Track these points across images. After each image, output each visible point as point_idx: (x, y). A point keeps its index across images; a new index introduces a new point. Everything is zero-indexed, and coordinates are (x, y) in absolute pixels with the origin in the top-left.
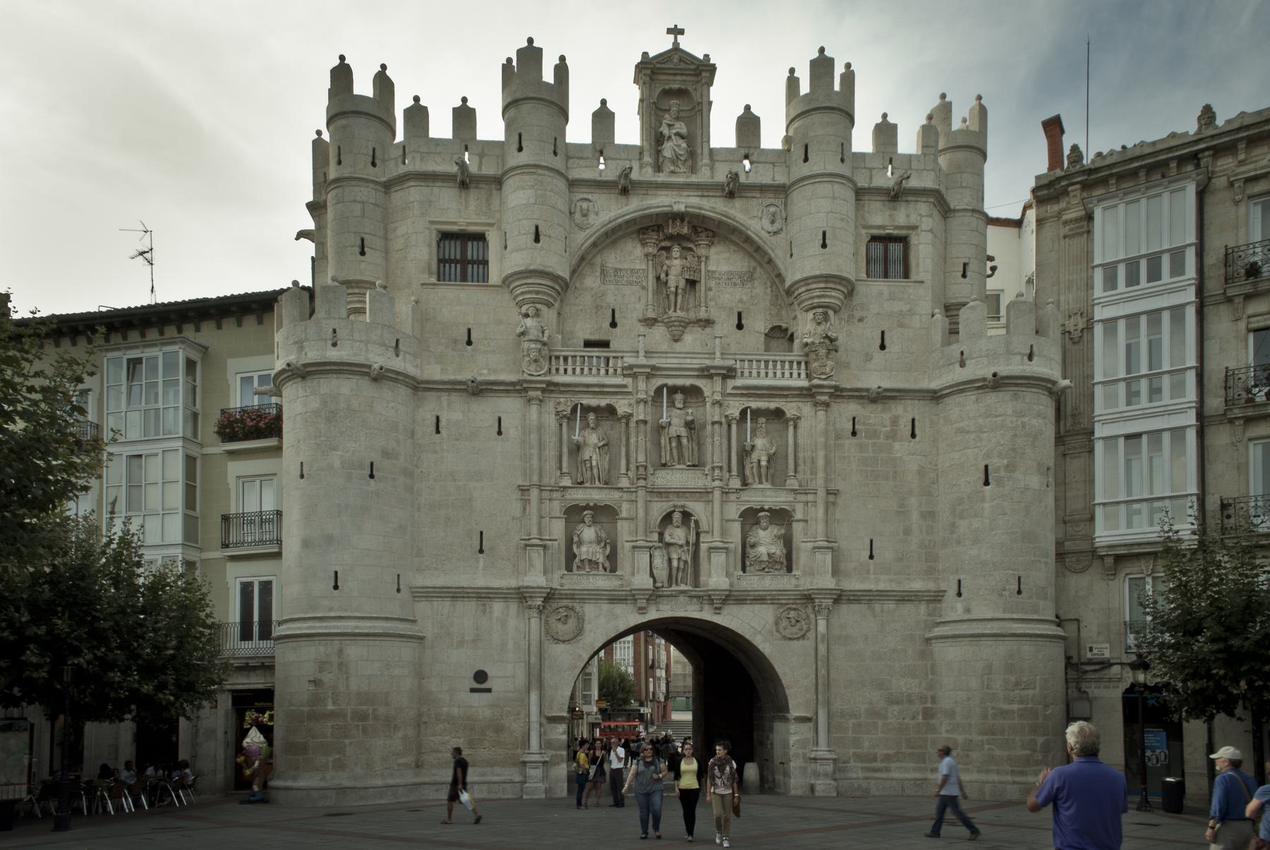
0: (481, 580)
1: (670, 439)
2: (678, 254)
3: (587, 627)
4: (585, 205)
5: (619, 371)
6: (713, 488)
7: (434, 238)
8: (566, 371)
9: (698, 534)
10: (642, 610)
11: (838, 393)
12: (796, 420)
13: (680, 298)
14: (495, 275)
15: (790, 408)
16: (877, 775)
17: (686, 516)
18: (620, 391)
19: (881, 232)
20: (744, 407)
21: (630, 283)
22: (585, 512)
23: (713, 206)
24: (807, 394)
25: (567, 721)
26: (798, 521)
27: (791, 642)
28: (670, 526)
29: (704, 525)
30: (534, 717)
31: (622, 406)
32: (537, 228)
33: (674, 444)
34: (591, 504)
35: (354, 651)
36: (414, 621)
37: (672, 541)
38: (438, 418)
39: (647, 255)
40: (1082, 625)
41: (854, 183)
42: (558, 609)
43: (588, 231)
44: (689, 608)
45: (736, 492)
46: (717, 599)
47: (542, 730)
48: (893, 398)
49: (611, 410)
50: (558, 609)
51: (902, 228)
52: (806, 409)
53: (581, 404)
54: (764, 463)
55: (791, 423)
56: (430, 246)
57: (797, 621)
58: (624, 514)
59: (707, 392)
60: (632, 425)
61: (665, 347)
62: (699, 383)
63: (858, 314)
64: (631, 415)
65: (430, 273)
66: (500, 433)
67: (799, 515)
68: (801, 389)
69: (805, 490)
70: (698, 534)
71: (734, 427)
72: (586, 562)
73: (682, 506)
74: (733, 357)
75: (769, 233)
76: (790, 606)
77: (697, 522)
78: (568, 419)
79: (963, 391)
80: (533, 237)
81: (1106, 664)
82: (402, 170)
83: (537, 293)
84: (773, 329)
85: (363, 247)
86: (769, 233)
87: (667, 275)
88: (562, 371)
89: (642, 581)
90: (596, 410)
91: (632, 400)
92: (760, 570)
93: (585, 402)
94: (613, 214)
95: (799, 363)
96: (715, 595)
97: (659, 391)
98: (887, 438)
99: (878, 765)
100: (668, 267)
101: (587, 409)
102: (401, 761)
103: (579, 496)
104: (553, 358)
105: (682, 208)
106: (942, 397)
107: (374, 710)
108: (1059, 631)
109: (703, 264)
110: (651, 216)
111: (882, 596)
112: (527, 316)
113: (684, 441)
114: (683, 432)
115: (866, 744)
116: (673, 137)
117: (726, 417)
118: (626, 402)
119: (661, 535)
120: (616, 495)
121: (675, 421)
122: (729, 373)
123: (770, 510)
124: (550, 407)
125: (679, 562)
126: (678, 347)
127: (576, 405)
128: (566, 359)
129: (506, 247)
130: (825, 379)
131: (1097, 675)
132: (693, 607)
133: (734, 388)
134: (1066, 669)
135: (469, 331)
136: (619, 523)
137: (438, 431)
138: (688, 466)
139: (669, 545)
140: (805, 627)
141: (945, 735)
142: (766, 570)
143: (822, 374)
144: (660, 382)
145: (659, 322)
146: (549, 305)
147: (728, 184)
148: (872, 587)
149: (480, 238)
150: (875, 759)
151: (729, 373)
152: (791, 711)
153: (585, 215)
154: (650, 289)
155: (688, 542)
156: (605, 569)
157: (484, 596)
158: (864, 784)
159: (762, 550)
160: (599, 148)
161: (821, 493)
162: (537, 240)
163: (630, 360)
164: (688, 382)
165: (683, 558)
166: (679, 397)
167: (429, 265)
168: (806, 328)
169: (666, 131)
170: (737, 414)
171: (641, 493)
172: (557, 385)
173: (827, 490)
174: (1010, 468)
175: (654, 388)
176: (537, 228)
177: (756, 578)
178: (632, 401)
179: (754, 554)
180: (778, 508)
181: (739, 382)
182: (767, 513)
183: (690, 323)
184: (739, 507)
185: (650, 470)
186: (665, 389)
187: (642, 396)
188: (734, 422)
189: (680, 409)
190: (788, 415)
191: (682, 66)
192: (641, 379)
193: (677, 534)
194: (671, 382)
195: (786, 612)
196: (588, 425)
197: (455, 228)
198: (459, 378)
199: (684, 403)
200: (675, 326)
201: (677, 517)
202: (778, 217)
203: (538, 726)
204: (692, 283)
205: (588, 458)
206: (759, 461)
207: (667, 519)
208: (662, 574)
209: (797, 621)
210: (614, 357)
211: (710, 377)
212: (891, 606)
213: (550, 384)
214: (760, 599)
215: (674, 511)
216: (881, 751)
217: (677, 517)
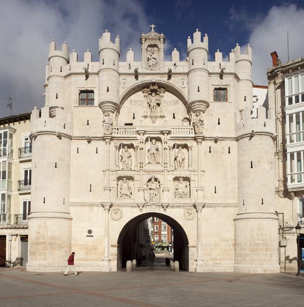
0: (90, 200)
3: (123, 216)
4: (124, 80)
7: (78, 92)
9: (160, 185)
11: (204, 139)
14: (96, 103)
15: (189, 143)
16: (217, 265)
17: (156, 180)
18: (135, 139)
19: (218, 87)
21: (139, 105)
23: (164, 80)
24: (195, 139)
27: (190, 221)
30: (107, 245)
31: (135, 143)
33: (152, 155)
35: (49, 222)
36: (70, 214)
38: (78, 148)
40: (284, 215)
41: (208, 72)
48: (223, 140)
51: (224, 85)
52: (194, 143)
54: (181, 162)
56: (76, 95)
58: (135, 179)
60: (139, 148)
61: (150, 125)
62: (160, 136)
63: (211, 113)
65: (76, 103)
66: (97, 153)
67: (192, 179)
68: (192, 137)
70: (160, 185)
79: (244, 137)
81: (291, 228)
82: (69, 72)
84: (184, 119)
85: (57, 96)
88: (116, 133)
89: (141, 201)
91: (139, 142)
93: (124, 143)
94: (133, 84)
95: (192, 129)
98: (221, 153)
99: (217, 262)
102: (64, 258)
103: (122, 174)
105: (154, 81)
106: (239, 140)
107: (55, 242)
108: (276, 217)
110: (145, 83)
111: (219, 205)
113: (155, 155)
114: (155, 152)
115: (214, 255)
119: (147, 185)
121: (152, 148)
122: (169, 133)
123: (183, 177)
124: (113, 143)
126: (154, 125)
128: (118, 129)
131: (289, 231)
132: (157, 209)
134: (279, 229)
137: (78, 153)
139: (150, 189)
141: (238, 252)
144: (147, 136)
146: (113, 113)
148: (216, 203)
149: (92, 92)
150: (216, 260)
151: (169, 133)
152: (189, 244)
153: (124, 84)
157: (92, 205)
158: (213, 268)
159: (180, 191)
161: (200, 171)
163: (138, 129)
164: (156, 136)
166: (154, 141)
167: (76, 101)
168: (194, 117)
169: (150, 58)
170: (172, 146)
171: (141, 171)
172: (115, 137)
174: (259, 162)
181: (172, 135)
185: (144, 164)
187: (142, 140)
190: (189, 146)
191: (155, 37)
192: (141, 135)
193: (154, 185)
194: (151, 136)
197: (84, 89)
198: (85, 135)
201: (153, 180)
202: (185, 83)
204: (159, 105)
207: (150, 180)
208: (147, 199)
211: (163, 134)
212: (222, 209)
213: (112, 137)
214: (179, 207)
216: (219, 257)
217: (153, 180)
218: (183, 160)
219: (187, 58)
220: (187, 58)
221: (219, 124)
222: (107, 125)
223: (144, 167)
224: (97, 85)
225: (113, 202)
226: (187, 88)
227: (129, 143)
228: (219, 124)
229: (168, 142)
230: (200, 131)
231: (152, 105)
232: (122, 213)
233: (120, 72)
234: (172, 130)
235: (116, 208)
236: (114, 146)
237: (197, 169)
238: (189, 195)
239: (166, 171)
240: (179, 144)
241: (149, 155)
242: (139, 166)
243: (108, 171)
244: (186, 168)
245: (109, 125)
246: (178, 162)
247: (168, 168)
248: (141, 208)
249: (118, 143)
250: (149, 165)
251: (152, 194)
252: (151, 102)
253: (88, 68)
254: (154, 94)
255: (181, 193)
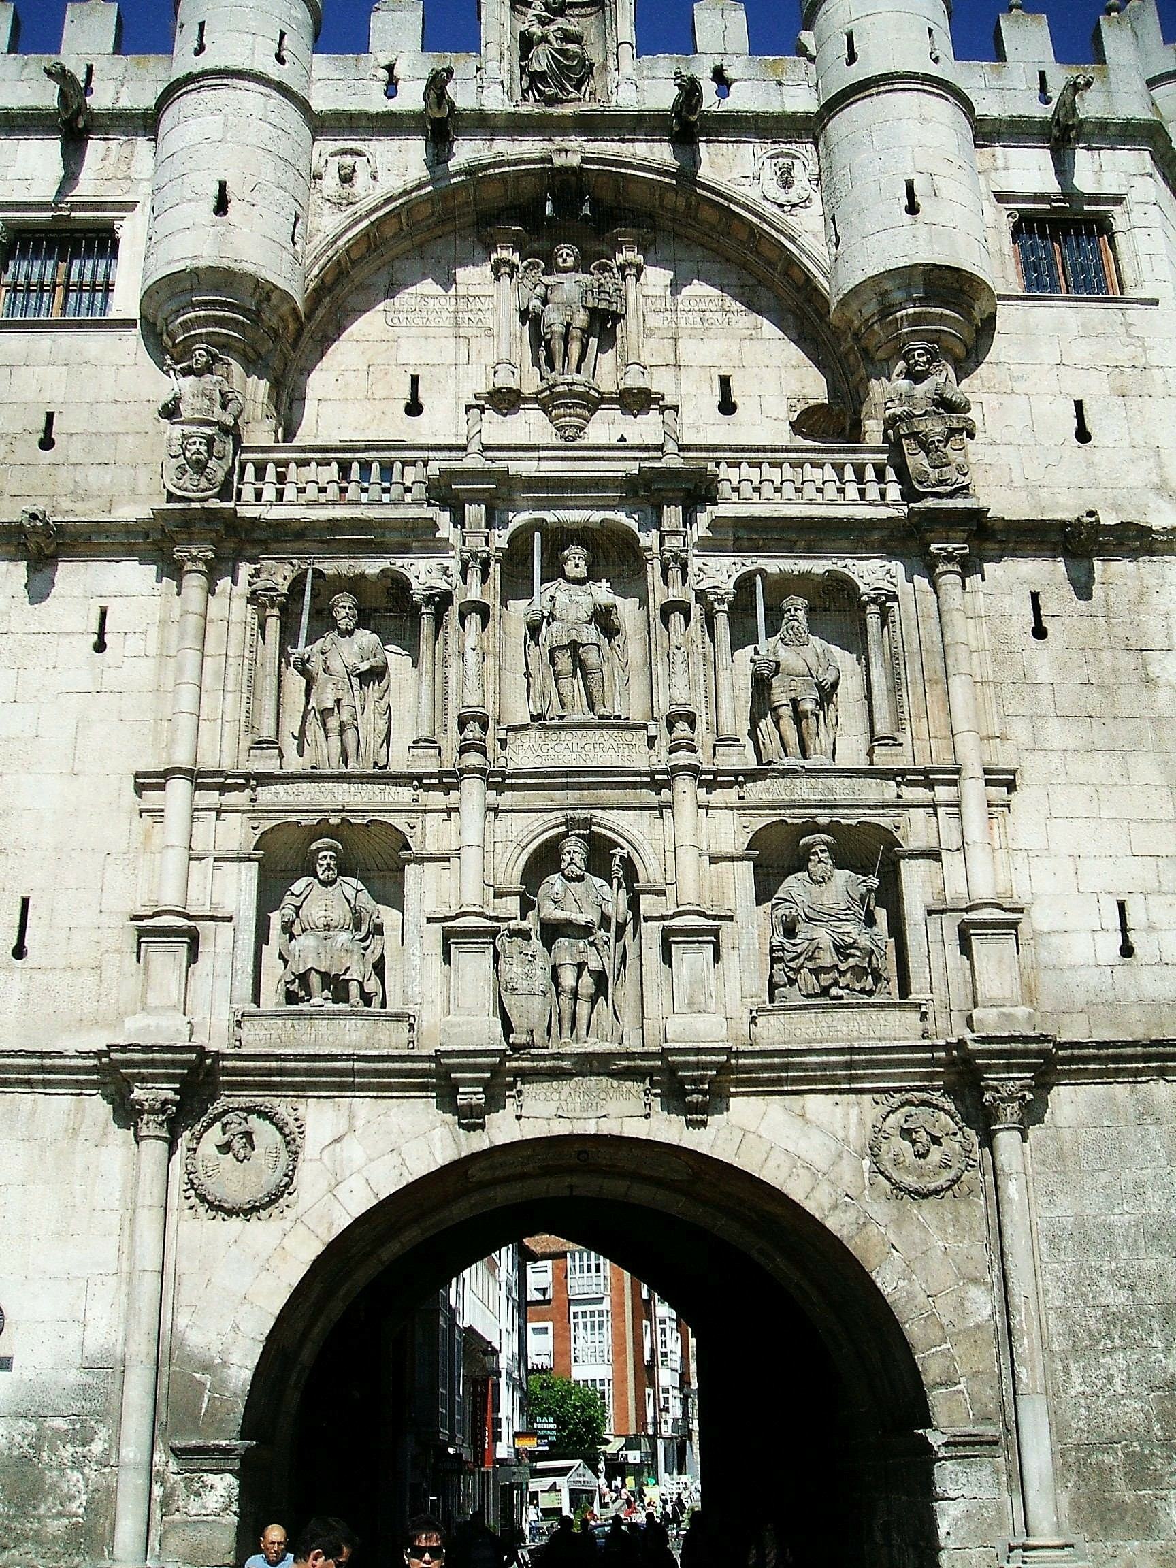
1: (552, 652)
2: (570, 262)
4: (348, 160)
5: (419, 492)
6: (675, 770)
8: (280, 494)
9: (634, 904)
10: (471, 1119)
12: (885, 601)
13: (575, 348)
20: (745, 569)
22: (314, 846)
25: (236, 1465)
26: (913, 855)
28: (555, 880)
29: (650, 870)
32: (223, 186)
33: (565, 662)
34: (334, 821)
37: (559, 915)
39: (496, 269)
42: (225, 1113)
43: (352, 209)
44: (613, 1107)
45: (737, 782)
46: (694, 1080)
47: (158, 1491)
49: (398, 585)
50: (225, 1113)
53: (318, 574)
55: (872, 608)
57: (936, 1141)
59: (649, 539)
64: (447, 598)
69: (926, 772)
70: (634, 904)
71: (722, 622)
72: (315, 980)
73: (588, 823)
74: (710, 454)
75: (781, 206)
76: (908, 1096)
77: (628, 864)
78: (284, 609)
80: (213, 203)
83: (219, 322)
86: (781, 206)
87: (545, 301)
88: (269, 494)
90: (355, 584)
92: (816, 995)
93: (328, 567)
96: (686, 1066)
97: (521, 539)
100: (547, 286)
101: (327, 586)
104: (250, 469)
105: (574, 160)
109: (631, 280)
112: (186, 372)
113: (591, 657)
114: (590, 634)
116: (551, 38)
117: (701, 596)
118: (434, 563)
120: (403, 795)
125: (579, 976)
127: (303, 575)
129: (150, 239)
130: (951, 495)
133: (715, 524)
135: (50, 416)
136: (411, 870)
138: (602, 717)
139: (551, 932)
140: (957, 1165)
142: (834, 991)
143: (942, 482)
145: (526, 400)
147: (678, 115)
153: (347, 179)
154: (504, 335)
155: (605, 920)
156: (367, 999)
160: (385, 62)
162: (222, 206)
164: (597, 516)
165: (594, 964)
169: (537, 30)
171: (473, 787)
173: (986, 771)
175: (506, 533)
176: (223, 186)
177: (808, 1015)
178: (446, 563)
179: (799, 949)
180: (854, 822)
182: (825, 837)
183: (603, 400)
184: (745, 821)
186: (537, 535)
188: (725, 607)
189: (580, 581)
190: (863, 589)
194: (549, 516)
195: (899, 1116)
196: (333, 626)
199: (590, 565)
200: (565, 405)
201: (574, 851)
202: (799, 174)
203: (141, 1481)
205: (330, 704)
206: (795, 703)
209: (936, 1141)
210: (405, 464)
215: (565, 835)
217: (574, 851)
218: (827, 694)
219: (807, 38)
220: (807, 38)
221: (1083, 435)
222: (193, 429)
223: (491, 742)
224: (146, 187)
225: (217, 1042)
226: (816, 206)
227: (372, 567)
228: (1083, 435)
229: (694, 564)
230: (951, 473)
231: (554, 318)
232: (291, 1142)
233: (318, 104)
234: (725, 472)
235: (243, 1099)
236: (243, 588)
237: (944, 759)
238: (892, 971)
239: (685, 785)
240: (785, 578)
241: (538, 656)
242: (451, 740)
243: (179, 788)
244: (852, 753)
245: (208, 430)
246: (786, 712)
247: (702, 758)
248: (470, 1096)
249: (279, 575)
250: (535, 736)
251: (568, 978)
252: (545, 301)
253: (88, 90)
254: (567, 254)
255: (827, 958)
